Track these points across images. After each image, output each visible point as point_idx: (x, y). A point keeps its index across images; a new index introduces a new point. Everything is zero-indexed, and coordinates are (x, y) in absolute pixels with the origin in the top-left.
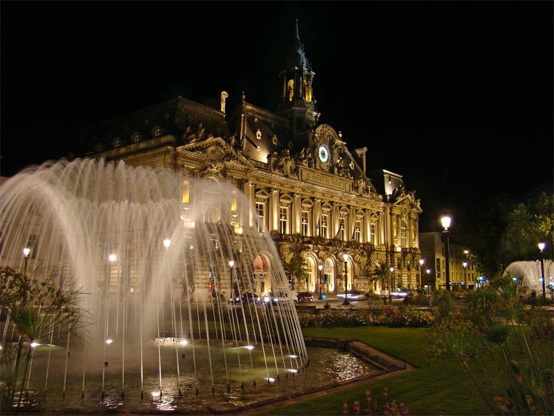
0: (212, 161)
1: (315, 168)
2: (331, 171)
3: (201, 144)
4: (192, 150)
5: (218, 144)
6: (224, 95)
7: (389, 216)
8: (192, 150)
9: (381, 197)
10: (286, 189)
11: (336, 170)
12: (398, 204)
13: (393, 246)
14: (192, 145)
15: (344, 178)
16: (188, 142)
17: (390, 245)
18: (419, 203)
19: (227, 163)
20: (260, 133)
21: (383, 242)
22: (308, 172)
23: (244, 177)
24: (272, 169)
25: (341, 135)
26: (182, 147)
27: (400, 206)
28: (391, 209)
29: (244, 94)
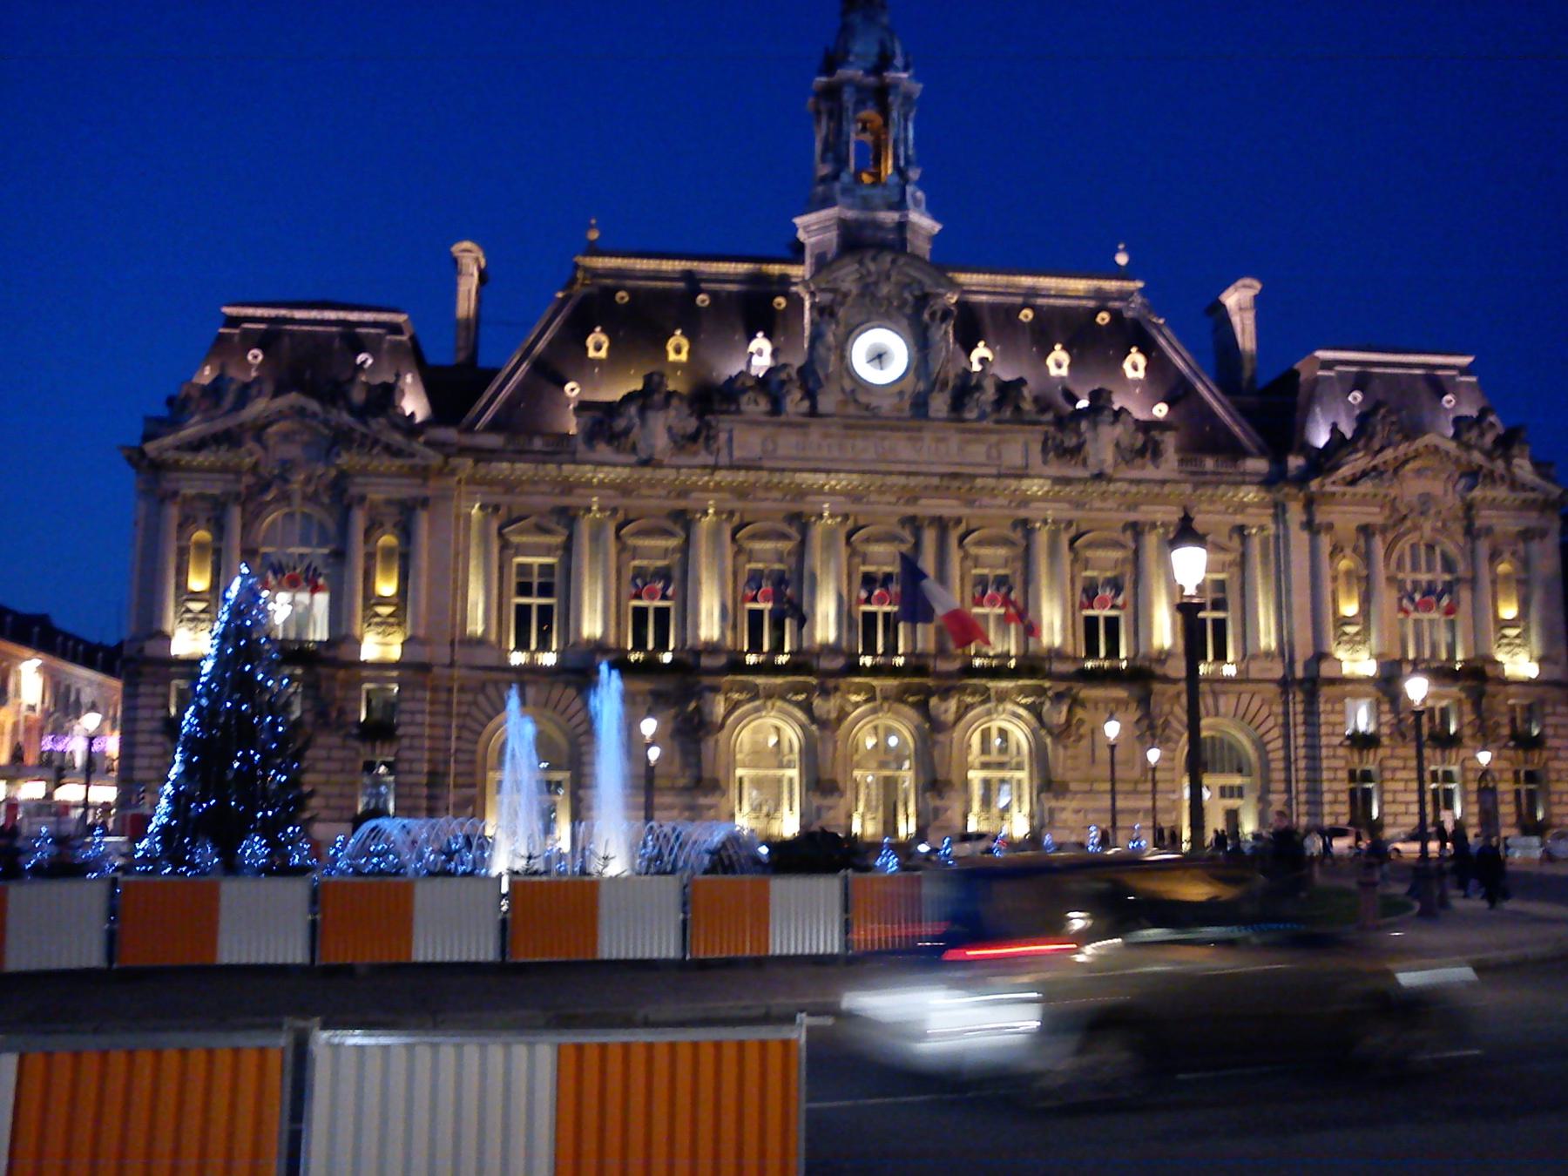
1: (813, 412)
2: (920, 405)
4: (197, 446)
5: (301, 412)
6: (470, 257)
7: (1299, 540)
8: (197, 446)
10: (654, 503)
11: (939, 404)
12: (1353, 481)
13: (1320, 656)
15: (985, 424)
17: (1303, 652)
19: (338, 462)
21: (1273, 645)
22: (768, 430)
25: (1122, 259)
27: (1365, 487)
28: (1309, 504)
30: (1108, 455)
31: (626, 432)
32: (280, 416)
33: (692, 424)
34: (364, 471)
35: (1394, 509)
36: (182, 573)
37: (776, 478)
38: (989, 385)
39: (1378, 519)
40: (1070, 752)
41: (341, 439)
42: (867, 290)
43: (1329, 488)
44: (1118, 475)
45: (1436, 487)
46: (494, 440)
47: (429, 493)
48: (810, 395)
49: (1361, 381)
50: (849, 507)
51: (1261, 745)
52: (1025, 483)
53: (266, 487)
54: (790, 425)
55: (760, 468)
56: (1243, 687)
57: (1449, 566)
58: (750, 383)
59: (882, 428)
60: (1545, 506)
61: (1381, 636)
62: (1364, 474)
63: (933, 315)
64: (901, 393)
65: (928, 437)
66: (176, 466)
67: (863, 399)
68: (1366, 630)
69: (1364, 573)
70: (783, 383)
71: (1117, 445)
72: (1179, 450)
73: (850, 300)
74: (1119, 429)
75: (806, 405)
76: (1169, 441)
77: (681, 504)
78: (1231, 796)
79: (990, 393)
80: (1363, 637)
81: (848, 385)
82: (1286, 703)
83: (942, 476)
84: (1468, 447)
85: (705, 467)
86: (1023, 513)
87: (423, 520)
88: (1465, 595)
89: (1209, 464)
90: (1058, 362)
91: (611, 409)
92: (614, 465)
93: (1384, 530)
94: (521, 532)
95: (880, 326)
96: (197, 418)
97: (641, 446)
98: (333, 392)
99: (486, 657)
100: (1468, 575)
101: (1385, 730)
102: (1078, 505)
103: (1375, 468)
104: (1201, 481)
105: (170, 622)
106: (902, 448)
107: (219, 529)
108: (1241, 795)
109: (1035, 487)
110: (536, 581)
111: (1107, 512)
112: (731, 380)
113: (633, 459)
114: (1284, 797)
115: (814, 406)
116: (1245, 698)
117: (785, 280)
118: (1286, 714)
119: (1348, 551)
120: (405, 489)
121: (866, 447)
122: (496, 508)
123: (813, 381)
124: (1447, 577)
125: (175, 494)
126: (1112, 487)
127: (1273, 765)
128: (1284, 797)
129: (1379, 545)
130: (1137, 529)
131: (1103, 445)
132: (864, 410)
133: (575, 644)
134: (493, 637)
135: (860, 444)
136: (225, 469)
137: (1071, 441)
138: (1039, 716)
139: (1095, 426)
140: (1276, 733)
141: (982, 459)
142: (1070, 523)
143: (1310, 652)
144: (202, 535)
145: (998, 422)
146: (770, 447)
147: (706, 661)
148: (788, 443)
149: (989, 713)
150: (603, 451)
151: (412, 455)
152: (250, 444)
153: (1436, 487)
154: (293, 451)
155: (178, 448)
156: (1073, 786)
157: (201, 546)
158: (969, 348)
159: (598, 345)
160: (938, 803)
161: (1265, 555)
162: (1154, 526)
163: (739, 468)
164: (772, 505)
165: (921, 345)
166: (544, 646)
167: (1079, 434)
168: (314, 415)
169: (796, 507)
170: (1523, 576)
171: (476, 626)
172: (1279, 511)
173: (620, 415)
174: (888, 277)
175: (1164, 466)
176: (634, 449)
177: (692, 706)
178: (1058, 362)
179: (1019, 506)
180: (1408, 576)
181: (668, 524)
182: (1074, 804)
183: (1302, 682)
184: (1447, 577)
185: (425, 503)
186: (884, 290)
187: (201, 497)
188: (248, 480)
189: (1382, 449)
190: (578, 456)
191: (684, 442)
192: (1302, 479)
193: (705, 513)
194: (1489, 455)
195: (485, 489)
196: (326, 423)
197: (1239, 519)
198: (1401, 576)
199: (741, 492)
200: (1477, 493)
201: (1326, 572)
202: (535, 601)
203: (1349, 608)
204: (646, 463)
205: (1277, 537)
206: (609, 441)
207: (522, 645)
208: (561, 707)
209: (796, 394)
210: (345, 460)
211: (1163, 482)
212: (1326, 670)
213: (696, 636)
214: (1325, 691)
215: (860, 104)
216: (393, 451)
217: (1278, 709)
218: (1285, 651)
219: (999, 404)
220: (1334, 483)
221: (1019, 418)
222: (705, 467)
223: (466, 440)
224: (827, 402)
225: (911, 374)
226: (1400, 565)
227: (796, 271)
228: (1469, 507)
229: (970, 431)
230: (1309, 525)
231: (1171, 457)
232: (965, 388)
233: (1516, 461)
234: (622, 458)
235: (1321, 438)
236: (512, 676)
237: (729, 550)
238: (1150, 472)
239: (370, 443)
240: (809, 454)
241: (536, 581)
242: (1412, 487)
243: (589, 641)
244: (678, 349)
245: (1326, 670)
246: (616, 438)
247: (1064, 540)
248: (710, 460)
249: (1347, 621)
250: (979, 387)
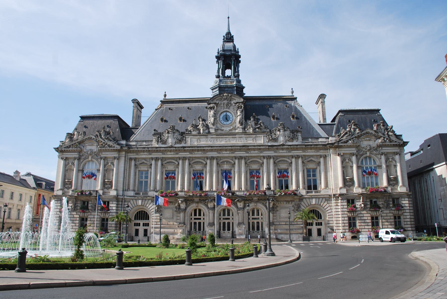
33: (179, 137)
40: (275, 215)
43: (340, 144)
44: (286, 144)
78: (319, 225)
83: (240, 146)
135: (221, 139)
175: (299, 141)
177: (176, 205)
198: (363, 166)
211: (297, 145)
220: (342, 143)
229: (248, 135)
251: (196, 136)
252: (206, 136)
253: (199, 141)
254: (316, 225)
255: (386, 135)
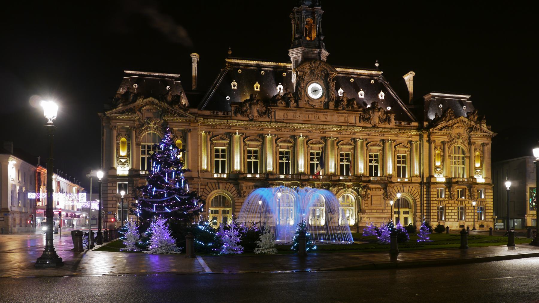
0: (148, 118)
1: (297, 107)
2: (326, 106)
3: (131, 106)
5: (153, 103)
7: (426, 145)
9: (415, 124)
11: (332, 105)
13: (431, 176)
14: (120, 108)
15: (344, 111)
16: (115, 106)
17: (426, 175)
18: (485, 125)
20: (236, 83)
21: (418, 174)
22: (285, 112)
23: (187, 127)
24: (233, 115)
26: (110, 112)
28: (429, 136)
29: (231, 50)
30: (377, 120)
31: (246, 111)
32: (146, 104)
34: (172, 121)
35: (451, 137)
36: (118, 150)
37: (288, 125)
38: (345, 99)
39: (447, 140)
41: (165, 112)
42: (312, 71)
43: (435, 131)
45: (462, 131)
46: (207, 113)
47: (191, 128)
48: (297, 101)
49: (442, 101)
50: (308, 134)
51: (414, 200)
52: (355, 128)
53: (143, 125)
54: (291, 110)
55: (283, 122)
56: (410, 185)
57: (463, 153)
58: (280, 98)
59: (316, 112)
60: (487, 137)
61: (446, 171)
62: (444, 127)
63: (330, 79)
64: (321, 102)
65: (329, 114)
66: (115, 118)
67: (311, 103)
68: (442, 169)
69: (442, 154)
70: (289, 98)
71: (379, 118)
72: (395, 120)
73: (307, 75)
74: (380, 113)
75: (296, 104)
76: (392, 117)
77: (261, 132)
79: (345, 103)
80: (441, 172)
81: (306, 99)
82: (421, 189)
84: (471, 120)
85: (268, 122)
86: (354, 136)
87: (189, 135)
88: (467, 161)
89: (403, 123)
90: (361, 94)
91: (241, 104)
92: (243, 121)
93: (448, 142)
94: (216, 140)
95: (315, 82)
96: (121, 104)
97: (250, 115)
98: (162, 97)
99: (208, 176)
100: (469, 155)
101: (447, 196)
102: (369, 135)
103: (447, 126)
104: (401, 128)
105: (116, 165)
106: (321, 117)
107: (129, 138)
108: (408, 214)
109: (357, 129)
110: (220, 153)
111: (376, 136)
112: (275, 97)
113: (248, 119)
114: (420, 214)
115: (298, 104)
116: (411, 187)
117: (285, 67)
118: (421, 192)
119: (438, 148)
120: (184, 127)
121: (312, 117)
122: (209, 132)
123: (295, 96)
124: (463, 156)
125: (116, 127)
126: (378, 130)
127: (418, 206)
128: (420, 214)
129: (447, 146)
130: (383, 141)
131: (376, 117)
132: (312, 107)
133: (233, 172)
134: (209, 170)
135: (310, 116)
136: (130, 120)
137: (367, 116)
138: (358, 192)
139: (373, 112)
140: (418, 197)
141: (343, 121)
142: (366, 139)
143: (428, 175)
144: (123, 139)
145: (347, 111)
146: (286, 116)
147: (270, 177)
148: (291, 115)
149: (345, 191)
150: (239, 116)
151: (186, 117)
152: (138, 112)
153: (462, 131)
154: (150, 115)
155: (116, 113)
156: (367, 211)
157: (123, 143)
158: (337, 89)
159: (234, 85)
160: (332, 216)
161: (417, 149)
162: (388, 140)
163: (278, 122)
164: (286, 133)
165: (327, 88)
166: (223, 172)
167: (369, 115)
168: (157, 104)
169: (293, 134)
170: (482, 156)
171: (205, 167)
172: (421, 137)
173: (244, 106)
174: (318, 68)
176: (248, 116)
178: (361, 94)
179: (353, 134)
180: (453, 155)
181: (258, 138)
182: (367, 216)
183: (426, 183)
184: (463, 156)
185: (190, 130)
186: (317, 71)
187: (123, 128)
188: (137, 123)
189: (449, 120)
190: (232, 118)
191: (261, 114)
192: (428, 128)
193: (268, 135)
194: (476, 122)
195: (206, 127)
196: (160, 107)
197: (410, 139)
199: (278, 129)
200: (472, 133)
201: (433, 154)
202: (220, 159)
203: (438, 163)
204: (251, 120)
205: (420, 144)
206: (241, 114)
207: (217, 172)
208: (229, 189)
209: (293, 102)
210: (167, 118)
211: (391, 128)
212: (432, 180)
213: (266, 170)
214: (432, 186)
215: (307, 16)
216: (180, 116)
217: (419, 191)
218: (421, 175)
219: (348, 105)
221: (353, 110)
222: (268, 122)
223: (200, 112)
224: (302, 104)
225: (324, 97)
226: (451, 153)
227: (288, 65)
228: (470, 137)
230: (429, 141)
231: (393, 122)
232: (338, 101)
233: (482, 125)
234: (244, 119)
235: (432, 117)
236: (216, 181)
237: (275, 145)
238: (388, 126)
239: (173, 113)
240: (297, 118)
241: (220, 153)
242: (456, 131)
243: (236, 171)
244: (257, 87)
245: (432, 180)
246: (243, 113)
247: (365, 143)
248: (269, 120)
249: (437, 167)
250: (342, 101)
251: (282, 109)
252: (293, 110)
253: (286, 116)
254: (404, 214)
255: (478, 125)
